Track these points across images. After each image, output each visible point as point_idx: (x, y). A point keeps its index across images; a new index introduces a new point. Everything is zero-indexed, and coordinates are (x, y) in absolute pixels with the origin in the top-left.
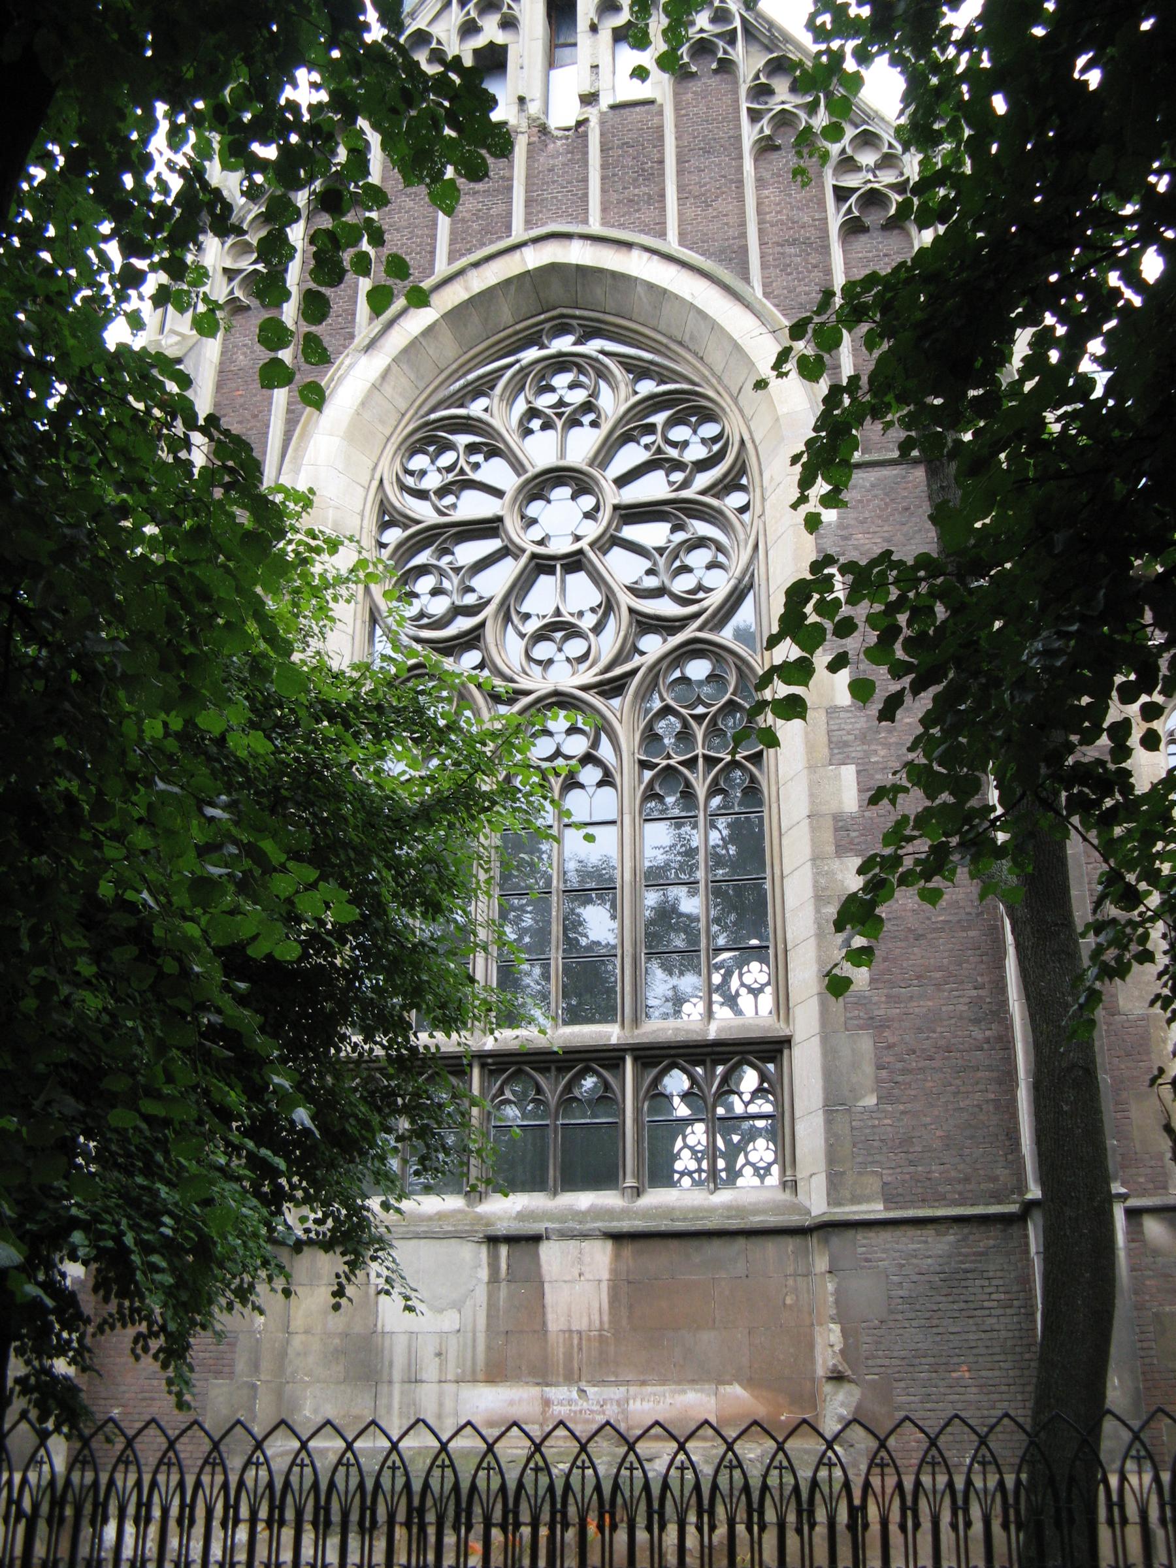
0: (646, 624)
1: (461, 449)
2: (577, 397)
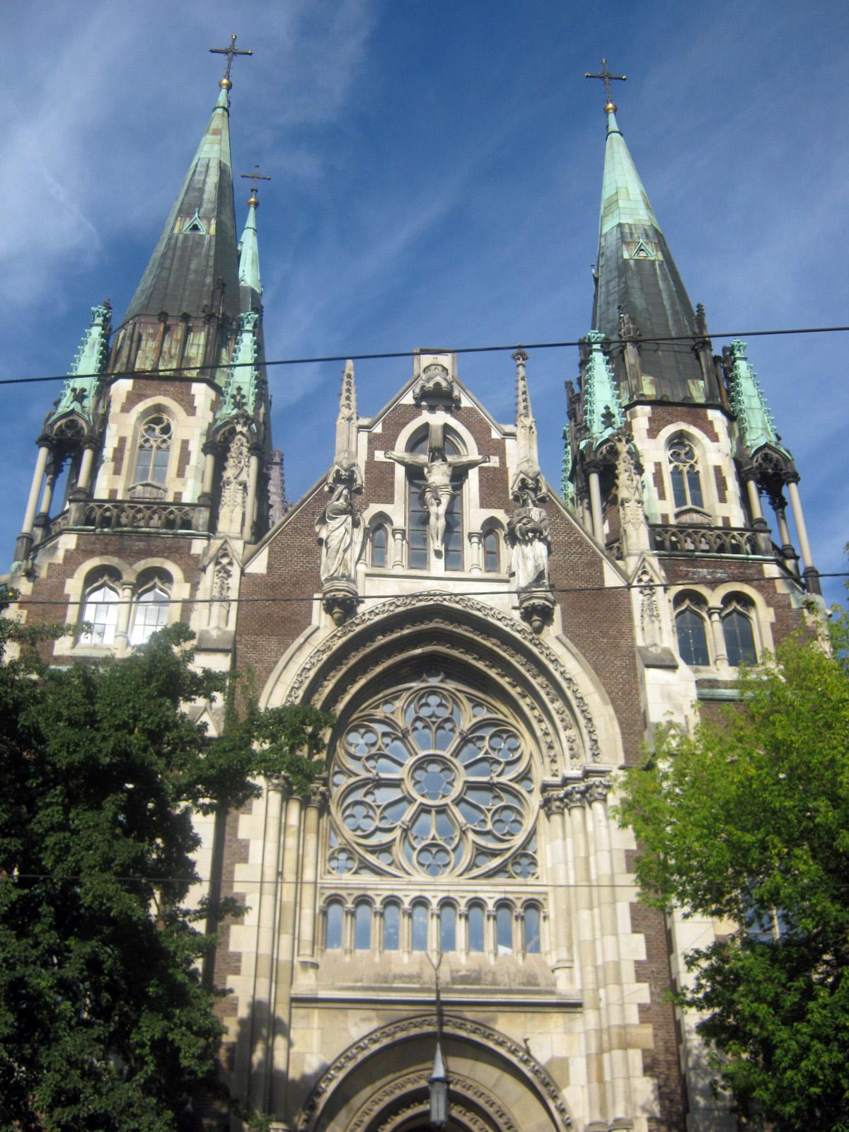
0: (482, 852)
1: (380, 735)
2: (444, 713)
